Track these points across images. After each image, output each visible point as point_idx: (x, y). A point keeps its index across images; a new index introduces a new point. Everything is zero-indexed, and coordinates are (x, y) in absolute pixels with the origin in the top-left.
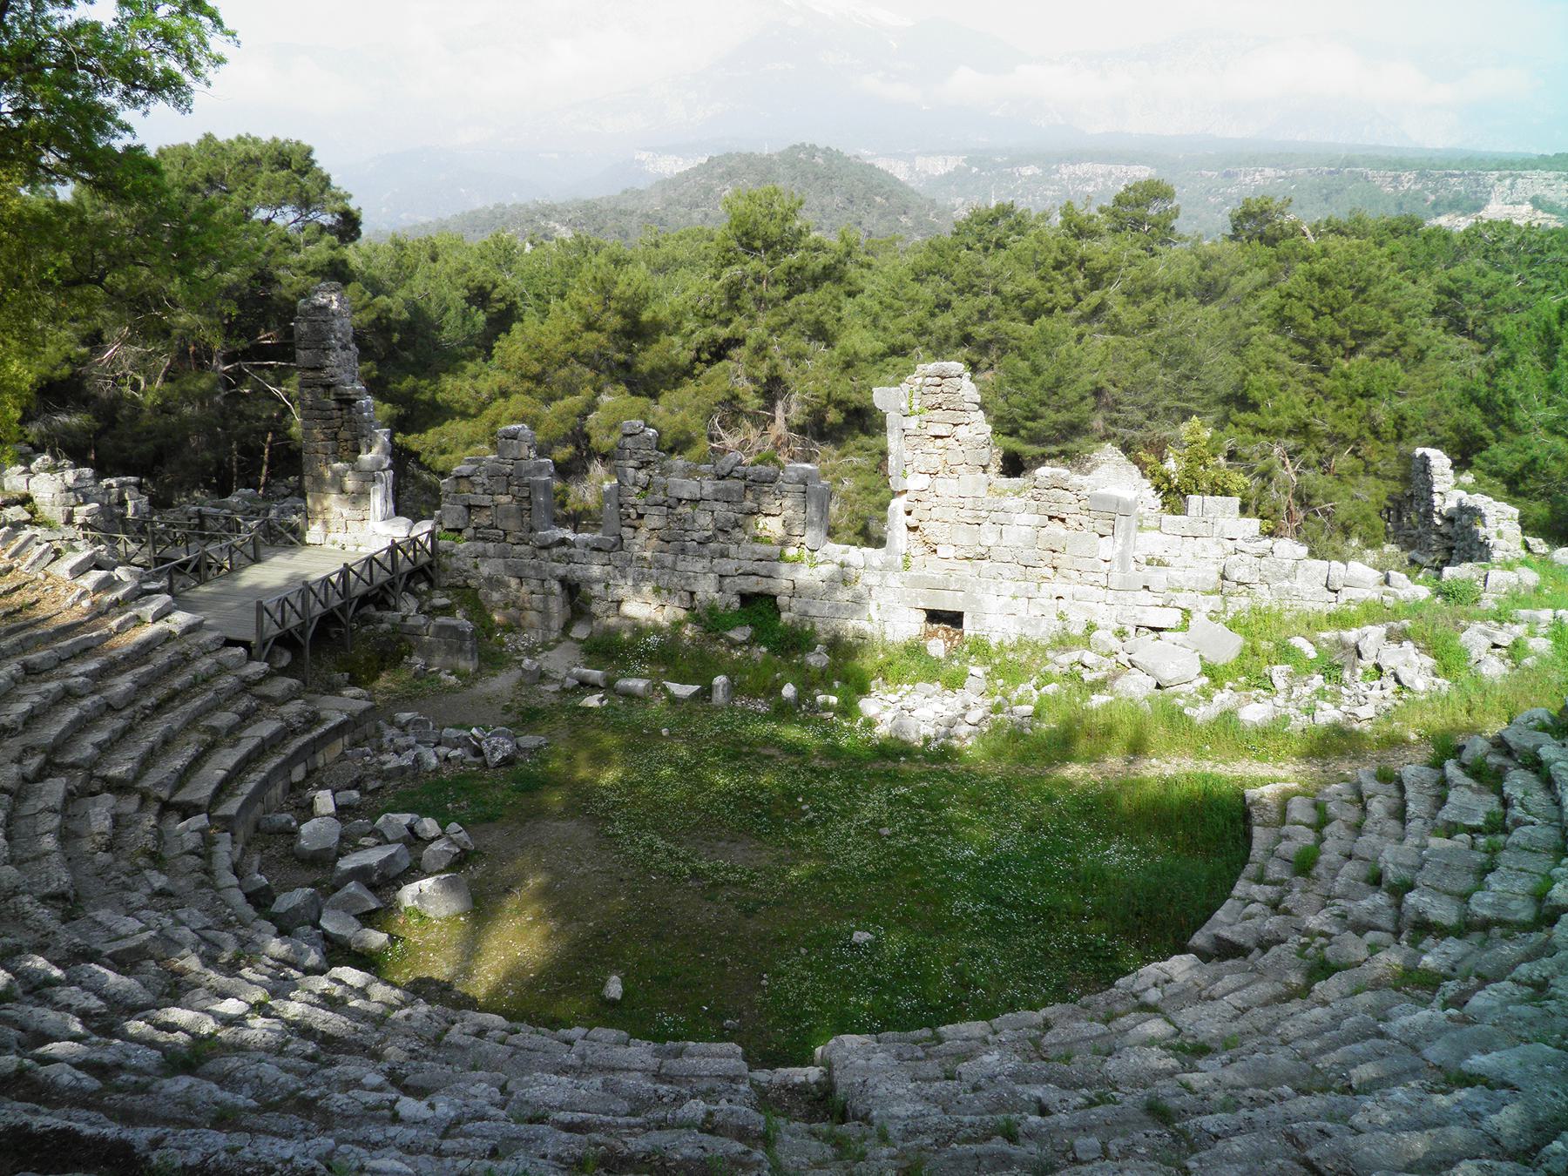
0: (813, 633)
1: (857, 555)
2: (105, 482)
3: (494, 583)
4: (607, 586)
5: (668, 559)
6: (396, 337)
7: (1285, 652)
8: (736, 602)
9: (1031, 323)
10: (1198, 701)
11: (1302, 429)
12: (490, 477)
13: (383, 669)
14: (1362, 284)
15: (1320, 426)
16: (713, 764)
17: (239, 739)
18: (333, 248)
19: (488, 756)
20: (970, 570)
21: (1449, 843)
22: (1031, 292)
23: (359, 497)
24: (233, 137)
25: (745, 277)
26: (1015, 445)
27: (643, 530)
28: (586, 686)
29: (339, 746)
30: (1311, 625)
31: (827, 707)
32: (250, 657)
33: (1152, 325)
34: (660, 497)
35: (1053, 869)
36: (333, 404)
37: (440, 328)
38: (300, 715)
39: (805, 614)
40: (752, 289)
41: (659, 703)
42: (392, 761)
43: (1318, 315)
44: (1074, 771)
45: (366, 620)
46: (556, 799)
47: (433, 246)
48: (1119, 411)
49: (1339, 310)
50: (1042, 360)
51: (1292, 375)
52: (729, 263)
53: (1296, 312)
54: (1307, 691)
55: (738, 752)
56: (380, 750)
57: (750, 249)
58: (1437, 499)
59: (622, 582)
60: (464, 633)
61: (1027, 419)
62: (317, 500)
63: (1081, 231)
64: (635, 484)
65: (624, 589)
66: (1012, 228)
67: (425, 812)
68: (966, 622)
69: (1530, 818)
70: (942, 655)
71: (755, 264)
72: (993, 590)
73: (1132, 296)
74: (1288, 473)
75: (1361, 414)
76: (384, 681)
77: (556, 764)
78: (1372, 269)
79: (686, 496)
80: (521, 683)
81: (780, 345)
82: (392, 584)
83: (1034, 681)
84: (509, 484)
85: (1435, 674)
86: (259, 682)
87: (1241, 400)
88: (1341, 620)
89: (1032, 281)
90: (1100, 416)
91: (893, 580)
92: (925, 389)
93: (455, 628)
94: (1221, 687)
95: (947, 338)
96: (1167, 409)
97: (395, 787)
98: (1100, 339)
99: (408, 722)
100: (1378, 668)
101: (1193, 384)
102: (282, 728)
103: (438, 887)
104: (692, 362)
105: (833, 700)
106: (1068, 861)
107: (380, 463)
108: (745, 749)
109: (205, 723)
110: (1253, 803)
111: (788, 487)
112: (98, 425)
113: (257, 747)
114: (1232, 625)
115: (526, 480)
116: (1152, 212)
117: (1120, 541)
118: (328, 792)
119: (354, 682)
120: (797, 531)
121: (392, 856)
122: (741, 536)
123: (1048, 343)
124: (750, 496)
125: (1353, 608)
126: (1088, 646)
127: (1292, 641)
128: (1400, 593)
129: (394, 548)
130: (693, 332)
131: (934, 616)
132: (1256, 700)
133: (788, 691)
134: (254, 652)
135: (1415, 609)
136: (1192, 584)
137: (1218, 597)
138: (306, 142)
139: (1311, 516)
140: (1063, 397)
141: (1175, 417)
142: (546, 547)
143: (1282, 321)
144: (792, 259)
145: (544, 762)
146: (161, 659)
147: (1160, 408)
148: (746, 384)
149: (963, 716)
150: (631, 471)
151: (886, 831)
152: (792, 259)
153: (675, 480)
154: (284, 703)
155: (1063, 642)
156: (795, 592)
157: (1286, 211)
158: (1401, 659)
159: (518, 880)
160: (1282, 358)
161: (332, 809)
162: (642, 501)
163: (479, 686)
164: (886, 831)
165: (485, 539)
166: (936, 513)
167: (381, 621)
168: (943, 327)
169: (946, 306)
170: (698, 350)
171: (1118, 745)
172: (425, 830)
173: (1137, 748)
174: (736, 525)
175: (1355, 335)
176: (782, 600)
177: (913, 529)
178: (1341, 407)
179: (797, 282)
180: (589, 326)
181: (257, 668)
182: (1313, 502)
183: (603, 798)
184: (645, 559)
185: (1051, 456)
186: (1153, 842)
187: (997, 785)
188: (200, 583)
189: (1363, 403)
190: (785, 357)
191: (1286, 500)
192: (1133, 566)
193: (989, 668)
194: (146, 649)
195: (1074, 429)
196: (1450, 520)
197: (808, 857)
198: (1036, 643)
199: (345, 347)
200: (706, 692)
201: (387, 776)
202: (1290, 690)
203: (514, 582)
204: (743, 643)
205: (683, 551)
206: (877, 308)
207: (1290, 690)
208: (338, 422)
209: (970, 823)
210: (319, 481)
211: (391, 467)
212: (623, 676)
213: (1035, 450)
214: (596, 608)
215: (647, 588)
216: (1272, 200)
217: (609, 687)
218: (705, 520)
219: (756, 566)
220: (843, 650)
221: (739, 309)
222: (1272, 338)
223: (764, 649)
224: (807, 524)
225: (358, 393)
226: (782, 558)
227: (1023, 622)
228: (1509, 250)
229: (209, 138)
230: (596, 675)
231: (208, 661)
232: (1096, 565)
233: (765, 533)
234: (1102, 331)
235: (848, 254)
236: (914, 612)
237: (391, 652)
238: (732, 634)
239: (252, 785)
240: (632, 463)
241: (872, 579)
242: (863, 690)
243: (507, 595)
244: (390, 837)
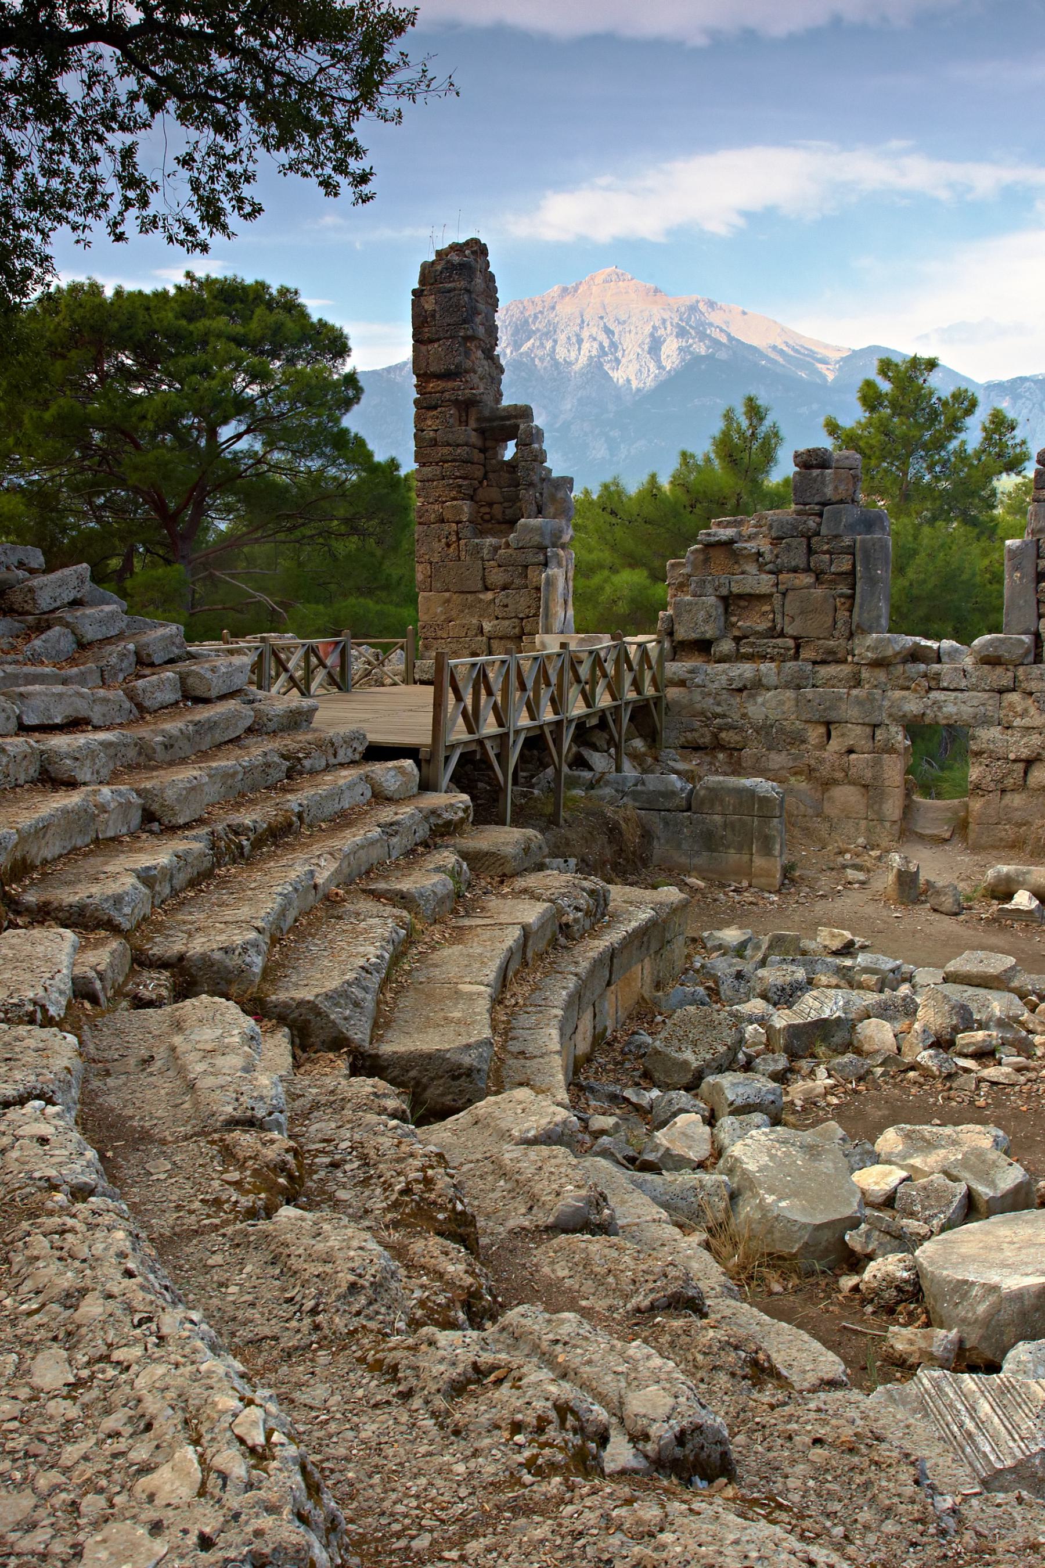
12: (776, 541)
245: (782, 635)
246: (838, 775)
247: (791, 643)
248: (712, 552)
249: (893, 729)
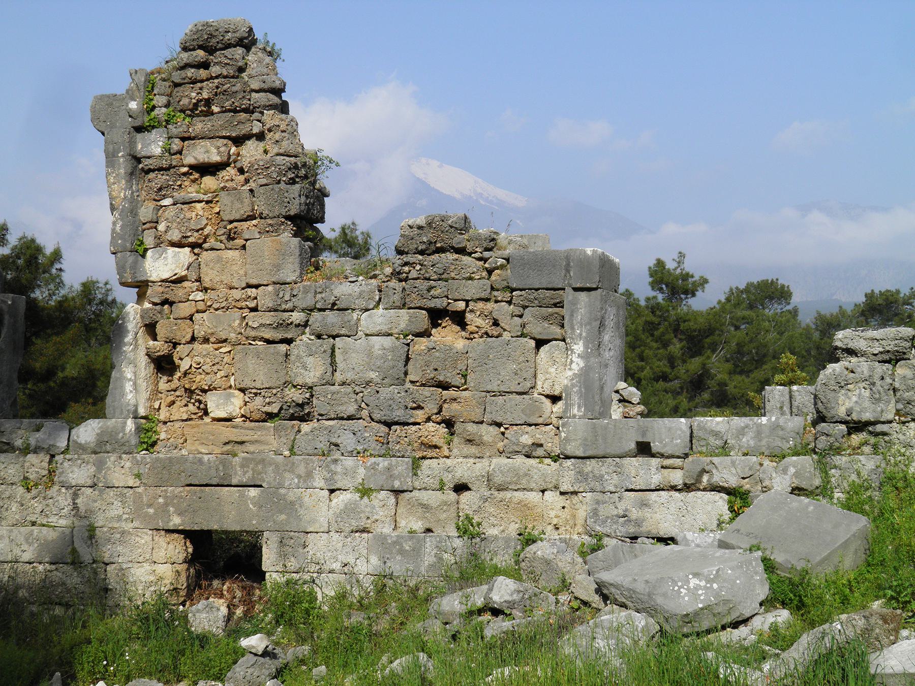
68: (269, 559)
72: (319, 482)
117: (579, 347)
166: (204, 324)
192: (616, 412)
227: (383, 545)
232: (536, 408)
236: (162, 540)
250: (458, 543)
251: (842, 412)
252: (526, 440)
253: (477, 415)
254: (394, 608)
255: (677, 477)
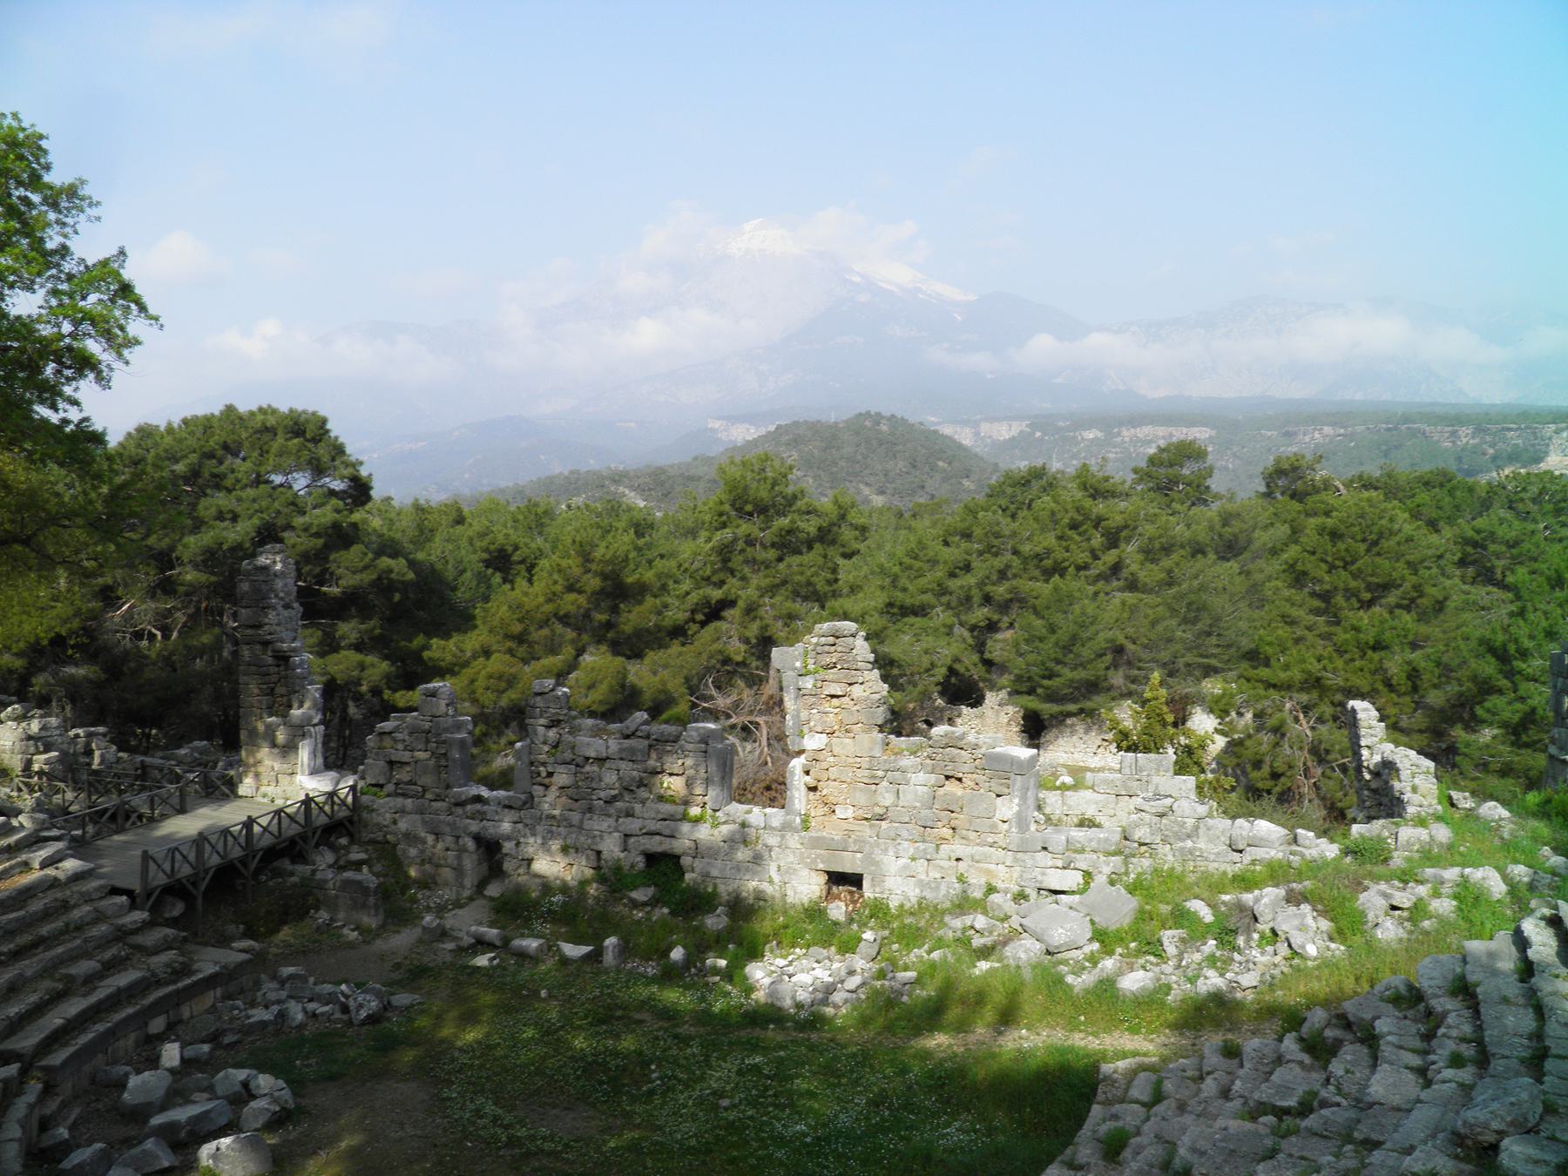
0: (715, 894)
1: (756, 815)
2: (72, 733)
3: (410, 838)
4: (518, 844)
5: (575, 817)
6: (397, 597)
7: (1181, 917)
8: (640, 862)
9: (1047, 581)
10: (1084, 968)
11: (1314, 683)
12: (411, 734)
13: (285, 923)
14: (1374, 537)
15: (1332, 680)
16: (580, 1027)
17: (95, 988)
18: (338, 511)
19: (353, 1014)
20: (868, 832)
21: (1249, 1126)
22: (1048, 552)
23: (289, 749)
24: (254, 408)
25: (735, 540)
26: (1033, 703)
27: (553, 788)
28: (481, 944)
29: (209, 998)
30: (1213, 886)
31: (716, 971)
32: (133, 906)
33: (1170, 582)
34: (568, 756)
35: (882, 1146)
36: (270, 660)
37: (455, 589)
38: (167, 965)
39: (706, 875)
40: (743, 551)
41: (548, 964)
42: (259, 1015)
43: (1332, 568)
44: (939, 1041)
45: (280, 873)
46: (408, 1056)
47: (459, 510)
48: (1139, 669)
49: (1353, 563)
50: (1058, 618)
51: (1309, 629)
52: (724, 526)
53: (1309, 566)
54: (1197, 957)
55: (608, 1016)
56: (253, 1004)
57: (743, 514)
58: (1365, 753)
59: (531, 840)
60: (368, 888)
61: (1044, 677)
62: (252, 753)
63: (1098, 490)
64: (545, 743)
65: (531, 845)
66: (1045, 490)
67: (262, 1068)
68: (866, 884)
69: (1338, 1099)
70: (842, 918)
71: (745, 528)
72: (891, 853)
73: (1150, 554)
74: (1303, 728)
75: (1372, 667)
76: (285, 933)
77: (423, 1022)
78: (1383, 522)
79: (593, 755)
80: (420, 941)
81: (772, 606)
82: (303, 837)
83: (926, 947)
84: (428, 741)
85: (1331, 939)
86: (136, 931)
87: (1254, 657)
88: (1245, 882)
89: (1050, 540)
90: (1121, 673)
91: (793, 841)
92: (819, 649)
93: (359, 883)
94: (1111, 953)
95: (968, 598)
96: (1188, 665)
97: (253, 1042)
98: (1119, 597)
99: (291, 977)
100: (1274, 932)
101: (1214, 640)
102: (144, 979)
103: (237, 1146)
104: (687, 622)
105: (722, 963)
106: (902, 1138)
107: (310, 718)
108: (619, 1013)
109: (64, 971)
110: (1106, 1078)
111: (690, 747)
112: (103, 676)
113: (109, 997)
114: (1132, 889)
115: (444, 737)
116: (1186, 471)
117: (1016, 801)
118: (176, 1046)
119: (250, 934)
120: (699, 790)
121: (206, 1113)
122: (646, 795)
123: (1063, 601)
124: (654, 755)
125: (1258, 868)
126: (985, 913)
127: (1188, 904)
128: (1307, 852)
129: (308, 801)
130: (688, 593)
131: (837, 879)
132: (1144, 968)
133: (677, 954)
134: (138, 900)
135: (1315, 868)
136: (1094, 845)
137: (1118, 859)
138: (322, 413)
139: (1328, 772)
140: (1078, 655)
141: (1197, 673)
142: (461, 804)
143: (1298, 578)
144: (784, 522)
145: (411, 1020)
146: (36, 906)
147: (1181, 662)
148: (738, 644)
149: (842, 982)
150: (541, 730)
151: (725, 1103)
152: (784, 522)
153: (583, 739)
154: (156, 953)
155: (964, 905)
156: (697, 850)
157: (1317, 466)
158: (1296, 922)
159: (332, 1140)
160: (1295, 612)
161: (176, 1062)
162: (552, 760)
163: (379, 942)
164: (725, 1103)
165: (404, 795)
166: (833, 773)
167: (292, 874)
168: (962, 587)
169: (967, 568)
170: (693, 612)
171: (989, 1014)
172: (258, 1087)
173: (1007, 1017)
174: (641, 784)
175: (1369, 588)
176: (686, 861)
177: (813, 789)
178: (1353, 660)
179: (788, 544)
180: (570, 588)
181: (139, 916)
182: (1330, 757)
183: (453, 1060)
184: (554, 817)
185: (1070, 715)
186: (1000, 1119)
187: (854, 1055)
188: (117, 832)
189: (1376, 656)
190: (776, 618)
191: (1302, 757)
192: (1033, 827)
193: (886, 933)
194: (28, 893)
195: (1093, 687)
196: (1376, 774)
197: (638, 1126)
198: (935, 907)
199: (287, 606)
200: (596, 956)
201: (250, 1030)
202: (1180, 957)
203: (430, 839)
204: (645, 904)
205: (590, 810)
206: (896, 569)
207: (1180, 957)
208: (274, 678)
209: (811, 1095)
210: (253, 733)
211: (322, 722)
212: (522, 936)
213: (1055, 708)
214: (508, 866)
215: (556, 845)
216: (1303, 457)
217: (504, 946)
218: (610, 778)
219: (658, 826)
220: (743, 910)
221: (732, 572)
222: (1287, 593)
223: (666, 910)
224: (708, 782)
225: (294, 650)
226: (685, 817)
228: (1534, 500)
229: (230, 409)
230: (493, 933)
231: (87, 908)
232: (994, 826)
233: (670, 793)
234: (1121, 590)
235: (843, 517)
236: (813, 874)
237: (298, 905)
238: (634, 895)
239: (91, 1036)
240: (542, 721)
241: (772, 840)
242: (755, 954)
243: (422, 852)
244: (219, 1093)
245: (415, 784)
246: (443, 862)
247: (420, 789)
248: (385, 737)
249: (467, 839)
250: (957, 885)
251: (1136, 838)
252: (990, 840)
253: (967, 827)
254: (927, 915)
255: (1060, 863)
